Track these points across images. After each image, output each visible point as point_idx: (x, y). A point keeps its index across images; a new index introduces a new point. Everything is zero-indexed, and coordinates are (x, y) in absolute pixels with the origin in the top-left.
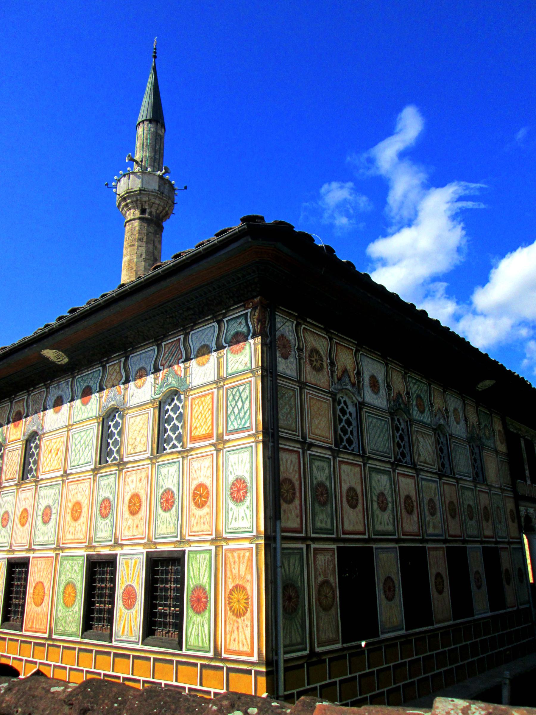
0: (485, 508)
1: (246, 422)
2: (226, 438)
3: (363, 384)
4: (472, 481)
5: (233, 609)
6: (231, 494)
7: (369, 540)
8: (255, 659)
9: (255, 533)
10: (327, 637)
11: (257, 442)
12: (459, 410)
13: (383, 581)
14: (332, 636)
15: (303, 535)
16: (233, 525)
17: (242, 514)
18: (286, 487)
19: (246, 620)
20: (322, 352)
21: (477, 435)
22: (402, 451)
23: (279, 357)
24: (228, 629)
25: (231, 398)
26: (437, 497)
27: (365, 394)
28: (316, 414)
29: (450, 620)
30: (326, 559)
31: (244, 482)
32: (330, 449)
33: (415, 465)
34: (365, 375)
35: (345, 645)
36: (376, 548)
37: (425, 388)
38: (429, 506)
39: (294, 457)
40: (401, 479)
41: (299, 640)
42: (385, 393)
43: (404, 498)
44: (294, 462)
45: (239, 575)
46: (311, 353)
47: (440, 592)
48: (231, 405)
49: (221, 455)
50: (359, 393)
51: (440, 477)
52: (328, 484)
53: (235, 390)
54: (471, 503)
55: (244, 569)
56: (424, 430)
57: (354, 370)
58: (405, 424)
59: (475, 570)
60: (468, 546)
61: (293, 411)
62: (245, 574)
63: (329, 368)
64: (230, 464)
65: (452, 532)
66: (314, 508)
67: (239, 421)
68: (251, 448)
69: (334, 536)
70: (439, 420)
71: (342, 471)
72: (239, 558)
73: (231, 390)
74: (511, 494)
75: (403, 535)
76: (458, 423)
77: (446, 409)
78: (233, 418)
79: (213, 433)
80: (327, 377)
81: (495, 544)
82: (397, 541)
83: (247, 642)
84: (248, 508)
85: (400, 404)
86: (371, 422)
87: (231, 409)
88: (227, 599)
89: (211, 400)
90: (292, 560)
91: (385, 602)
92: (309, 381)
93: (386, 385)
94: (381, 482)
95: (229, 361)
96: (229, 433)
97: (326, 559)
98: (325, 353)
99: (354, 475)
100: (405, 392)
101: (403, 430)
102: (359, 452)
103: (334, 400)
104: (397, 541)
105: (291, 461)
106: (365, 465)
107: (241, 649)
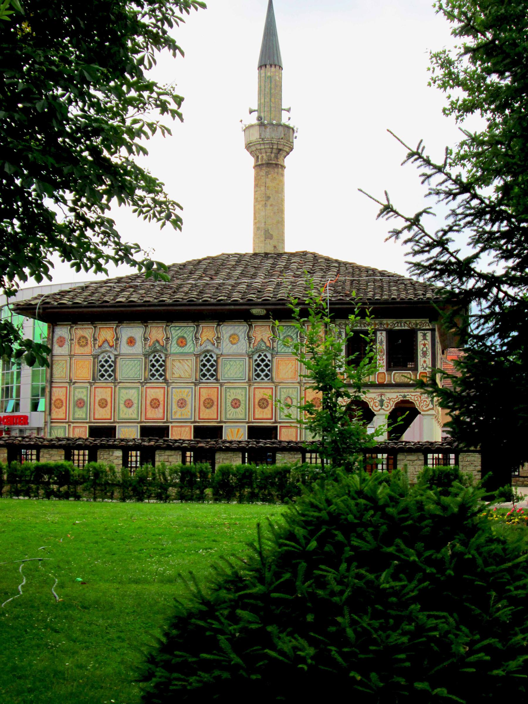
4: (247, 382)
7: (114, 422)
12: (240, 334)
15: (67, 420)
20: (87, 336)
21: (267, 347)
32: (89, 382)
37: (192, 329)
38: (178, 402)
50: (116, 349)
51: (196, 385)
52: (85, 398)
54: (239, 397)
56: (182, 358)
69: (88, 421)
94: (133, 394)
103: (94, 359)
106: (115, 386)
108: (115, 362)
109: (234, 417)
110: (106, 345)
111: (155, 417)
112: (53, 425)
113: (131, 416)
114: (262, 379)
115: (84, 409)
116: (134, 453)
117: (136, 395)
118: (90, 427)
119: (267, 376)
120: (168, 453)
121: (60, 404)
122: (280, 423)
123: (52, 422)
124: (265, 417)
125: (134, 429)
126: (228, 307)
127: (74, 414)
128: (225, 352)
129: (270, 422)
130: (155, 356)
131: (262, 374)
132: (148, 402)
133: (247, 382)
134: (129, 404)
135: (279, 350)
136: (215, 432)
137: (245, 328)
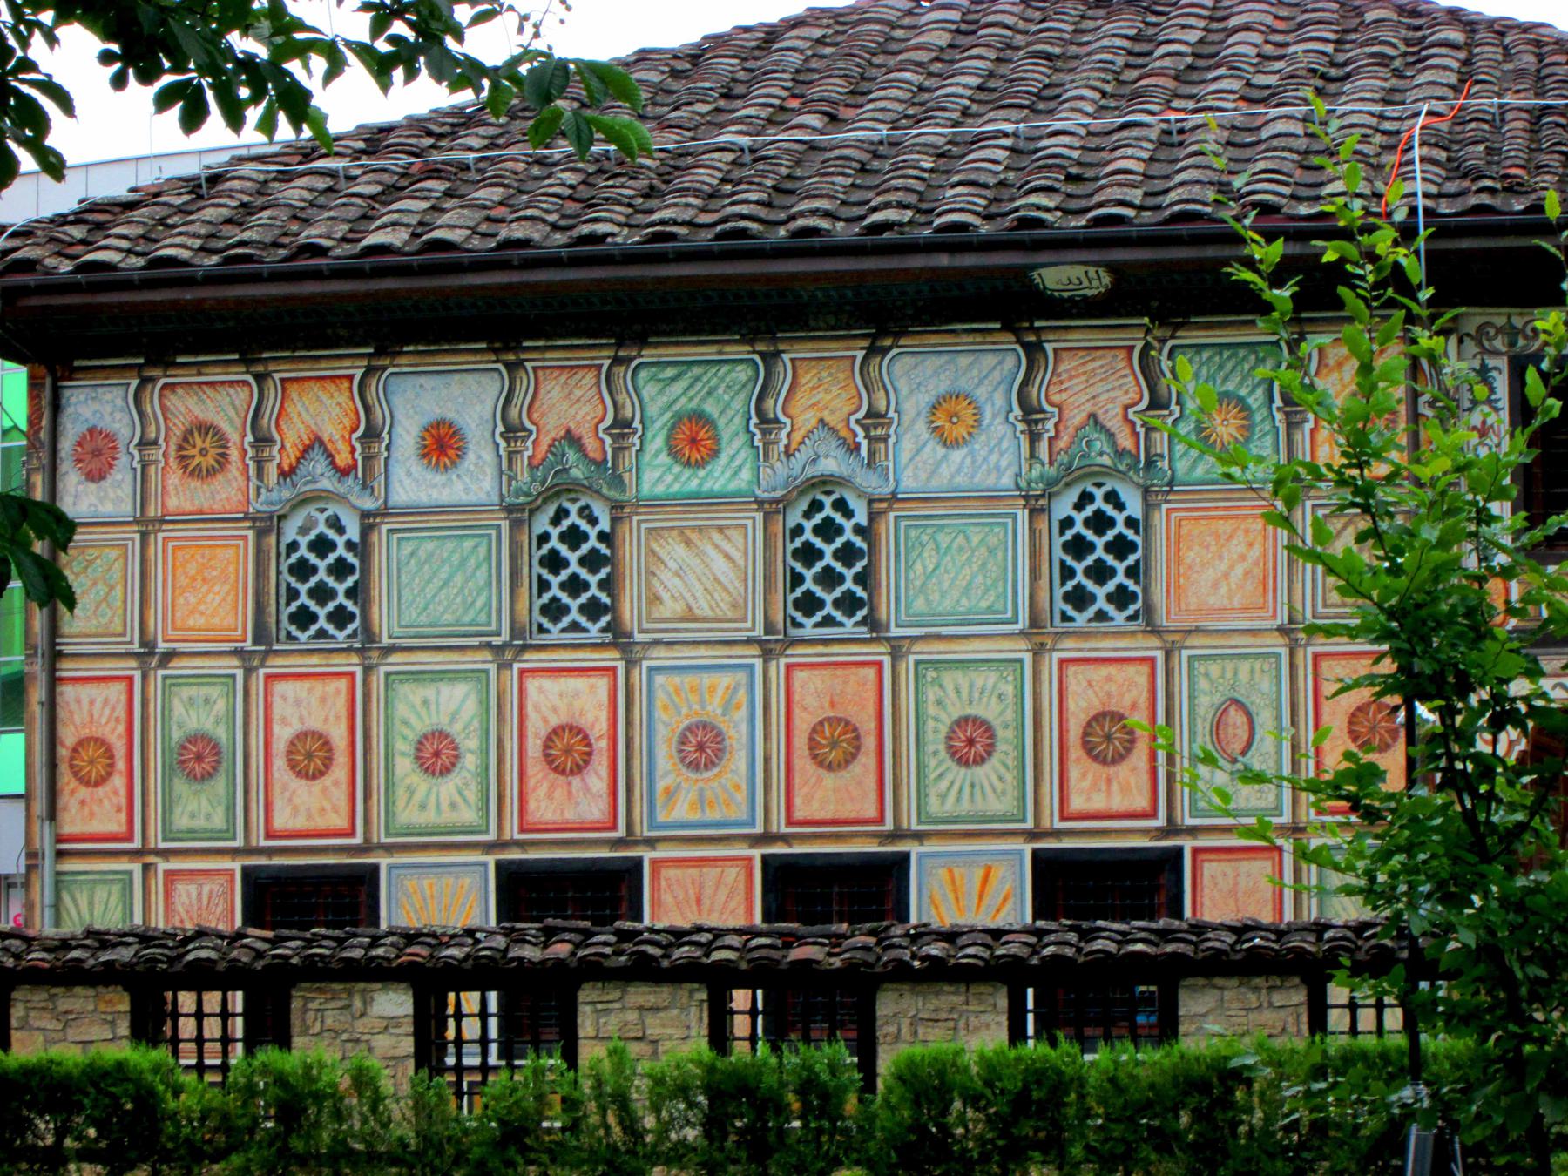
12: (981, 393)
15: (137, 844)
20: (226, 427)
21: (1120, 454)
26: (742, 713)
32: (237, 653)
34: (398, 430)
36: (391, 867)
37: (742, 373)
38: (683, 741)
39: (116, 691)
42: (488, 456)
43: (544, 732)
46: (185, 439)
52: (221, 734)
54: (988, 710)
56: (700, 518)
57: (354, 430)
60: (914, 849)
69: (239, 843)
80: (241, 480)
82: (489, 847)
93: (500, 428)
98: (238, 422)
99: (323, 700)
103: (261, 534)
104: (489, 847)
105: (106, 702)
106: (368, 670)
108: (362, 548)
109: (965, 807)
111: (569, 816)
112: (70, 865)
113: (448, 817)
114: (1101, 616)
115: (220, 784)
116: (471, 1001)
117: (471, 707)
118: (247, 872)
119: (1121, 598)
120: (640, 994)
121: (97, 763)
122: (1193, 831)
123: (60, 854)
124: (1118, 803)
125: (468, 881)
126: (917, 262)
127: (168, 810)
128: (910, 483)
129: (1145, 832)
130: (561, 514)
131: (1101, 592)
132: (534, 746)
133: (1022, 633)
134: (436, 755)
135: (1181, 466)
136: (875, 884)
137: (1010, 361)
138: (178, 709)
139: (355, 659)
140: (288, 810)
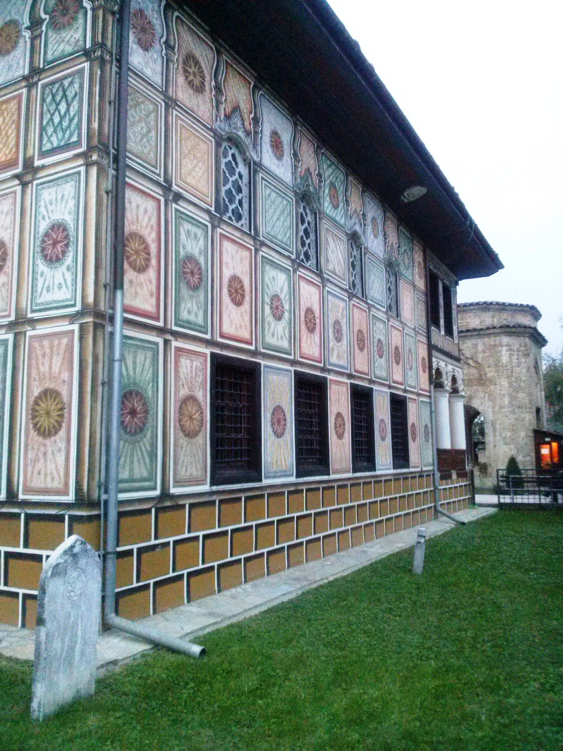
0: (397, 348)
1: (71, 135)
2: (38, 163)
3: (261, 138)
5: (38, 425)
6: (43, 250)
7: (255, 353)
8: (70, 498)
9: (78, 307)
10: (188, 474)
11: (88, 165)
13: (271, 411)
14: (196, 473)
15: (161, 324)
16: (45, 298)
17: (59, 279)
18: (133, 246)
19: (58, 441)
22: (307, 251)
23: (133, 41)
24: (30, 456)
25: (49, 99)
26: (345, 320)
27: (263, 153)
28: (190, 153)
29: (349, 472)
30: (194, 366)
31: (65, 229)
32: (208, 212)
33: (321, 272)
35: (215, 488)
38: (334, 328)
39: (150, 205)
40: (303, 284)
41: (145, 474)
42: (289, 162)
43: (305, 310)
44: (149, 213)
45: (50, 374)
47: (340, 436)
48: (49, 111)
49: (29, 191)
51: (351, 296)
52: (202, 260)
53: (57, 86)
54: (382, 338)
55: (58, 365)
56: (336, 232)
57: (251, 113)
58: (313, 216)
59: (380, 418)
61: (153, 134)
62: (60, 372)
63: (213, 93)
64: (42, 203)
65: (359, 367)
66: (179, 289)
67: (60, 135)
68: (77, 175)
69: (208, 337)
70: (355, 224)
71: (224, 249)
72: (51, 347)
73: (51, 87)
74: (424, 340)
75: (301, 357)
76: (376, 236)
77: (364, 215)
78: (50, 130)
79: (17, 159)
81: (404, 393)
82: (293, 363)
83: (59, 474)
84: (68, 269)
85: (308, 186)
86: (269, 195)
87: (49, 116)
88: (30, 412)
89: (16, 106)
90: (140, 357)
91: (272, 437)
92: (180, 99)
93: (292, 152)
94: (277, 281)
95: (50, 41)
96: (43, 154)
97: (194, 366)
98: (209, 69)
100: (317, 172)
101: (309, 223)
102: (250, 230)
105: (146, 211)
106: (256, 250)
107: (49, 486)
110: (239, 124)
138: (183, 236)
139: (252, 243)
140: (229, 322)
